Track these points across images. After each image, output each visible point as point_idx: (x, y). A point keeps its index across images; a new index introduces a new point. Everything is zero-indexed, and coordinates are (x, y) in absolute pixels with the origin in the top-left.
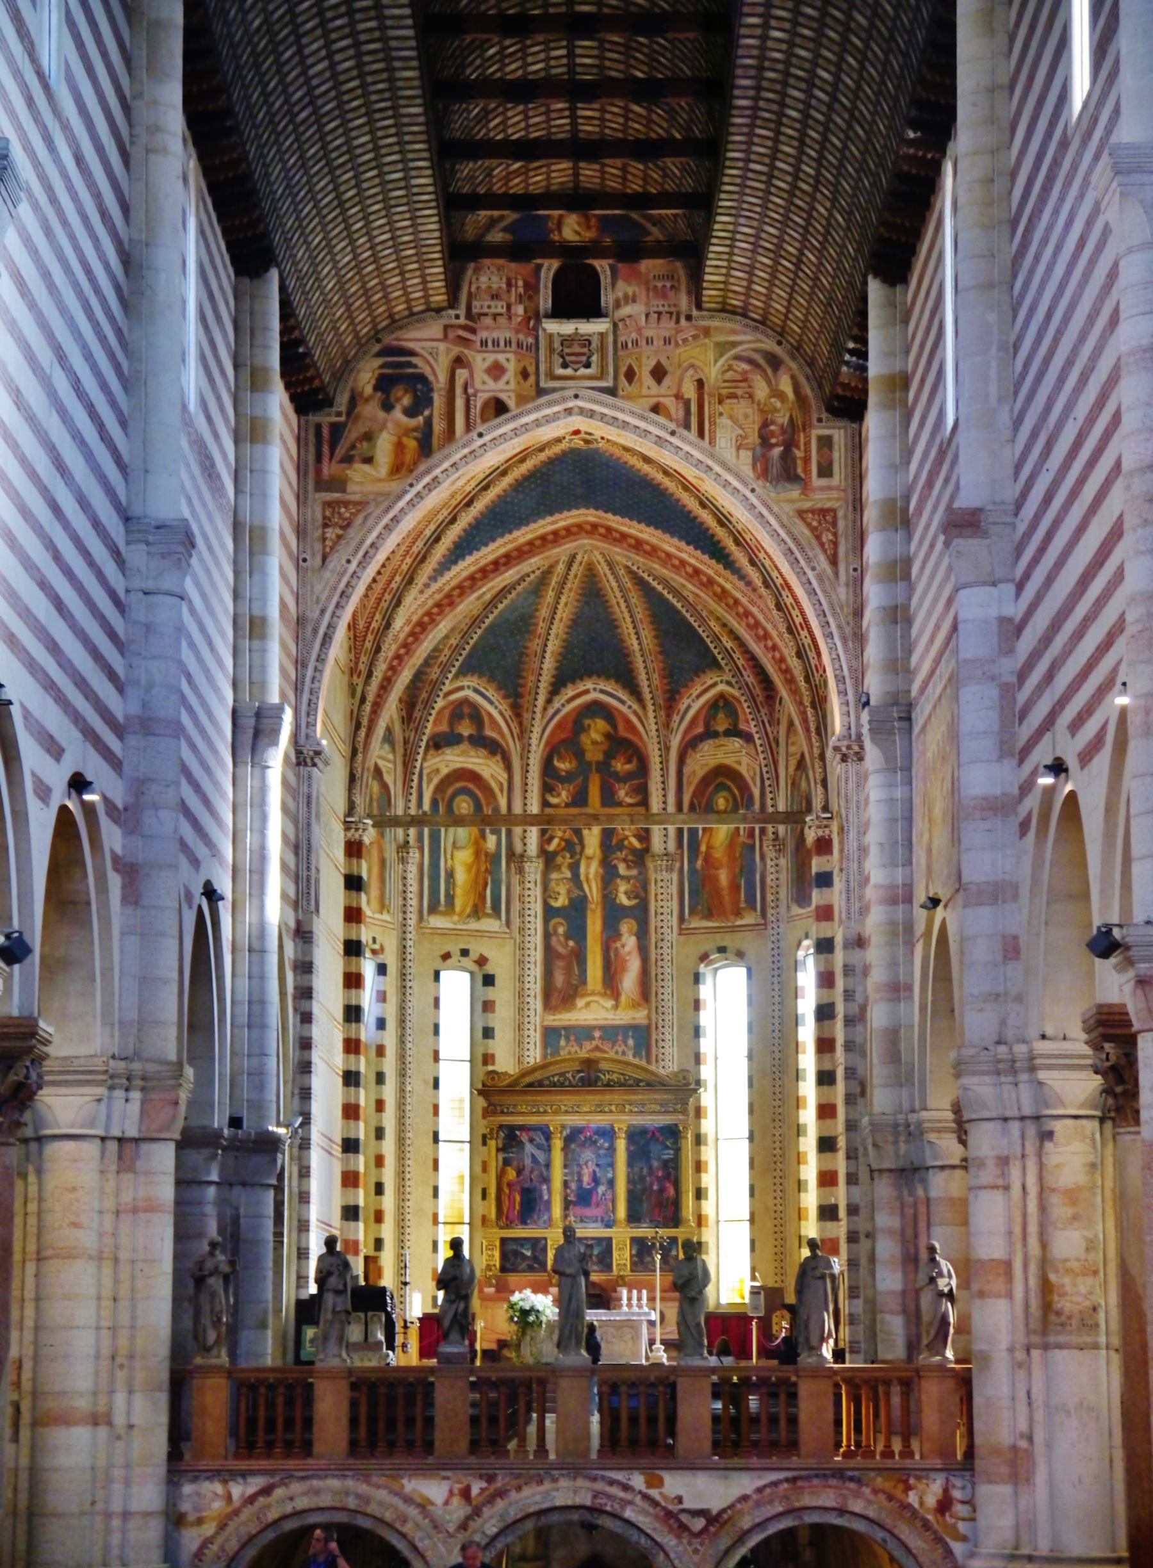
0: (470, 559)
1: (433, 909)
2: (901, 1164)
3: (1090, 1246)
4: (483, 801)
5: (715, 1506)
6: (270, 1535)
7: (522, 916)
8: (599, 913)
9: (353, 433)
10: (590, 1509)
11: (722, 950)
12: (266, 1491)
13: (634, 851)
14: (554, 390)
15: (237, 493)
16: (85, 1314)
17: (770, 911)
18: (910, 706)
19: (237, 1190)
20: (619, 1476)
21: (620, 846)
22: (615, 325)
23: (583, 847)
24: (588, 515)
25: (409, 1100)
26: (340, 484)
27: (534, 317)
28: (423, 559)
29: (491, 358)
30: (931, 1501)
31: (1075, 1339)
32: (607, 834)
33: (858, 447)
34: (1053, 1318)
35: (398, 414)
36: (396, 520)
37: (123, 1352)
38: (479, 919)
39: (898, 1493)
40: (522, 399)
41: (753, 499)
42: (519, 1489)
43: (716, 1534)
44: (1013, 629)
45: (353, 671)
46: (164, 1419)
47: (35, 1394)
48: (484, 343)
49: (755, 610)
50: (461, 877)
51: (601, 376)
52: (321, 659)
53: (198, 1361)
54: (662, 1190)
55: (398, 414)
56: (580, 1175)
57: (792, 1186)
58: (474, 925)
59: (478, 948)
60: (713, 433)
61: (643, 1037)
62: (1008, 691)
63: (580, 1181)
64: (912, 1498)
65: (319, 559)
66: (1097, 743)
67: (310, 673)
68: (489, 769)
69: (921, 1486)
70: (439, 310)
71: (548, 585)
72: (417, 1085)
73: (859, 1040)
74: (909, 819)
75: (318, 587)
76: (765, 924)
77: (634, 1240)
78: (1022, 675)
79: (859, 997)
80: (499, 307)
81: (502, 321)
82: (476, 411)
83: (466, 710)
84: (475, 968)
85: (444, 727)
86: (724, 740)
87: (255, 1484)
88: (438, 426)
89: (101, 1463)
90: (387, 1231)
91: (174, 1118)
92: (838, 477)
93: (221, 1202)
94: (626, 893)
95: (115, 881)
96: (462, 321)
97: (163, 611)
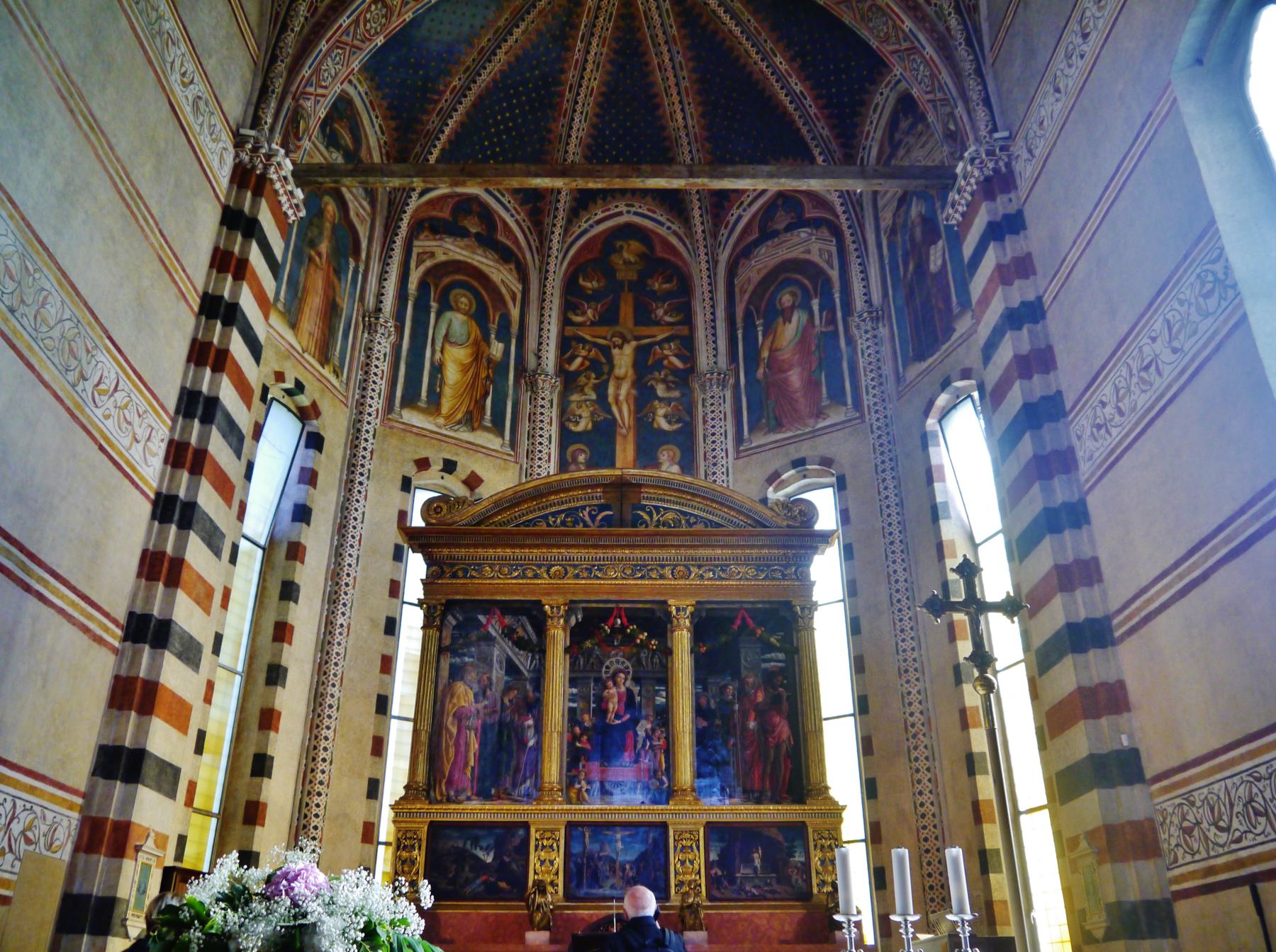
1: (410, 400)
4: (489, 304)
7: (531, 436)
8: (631, 437)
11: (799, 463)
13: (675, 371)
17: (867, 400)
21: (659, 365)
23: (612, 367)
25: (338, 638)
32: (642, 355)
38: (473, 429)
54: (766, 728)
56: (602, 702)
58: (465, 435)
63: (601, 711)
68: (501, 275)
71: (576, 27)
76: (862, 417)
83: (475, 207)
85: (445, 214)
86: (784, 237)
94: (665, 416)
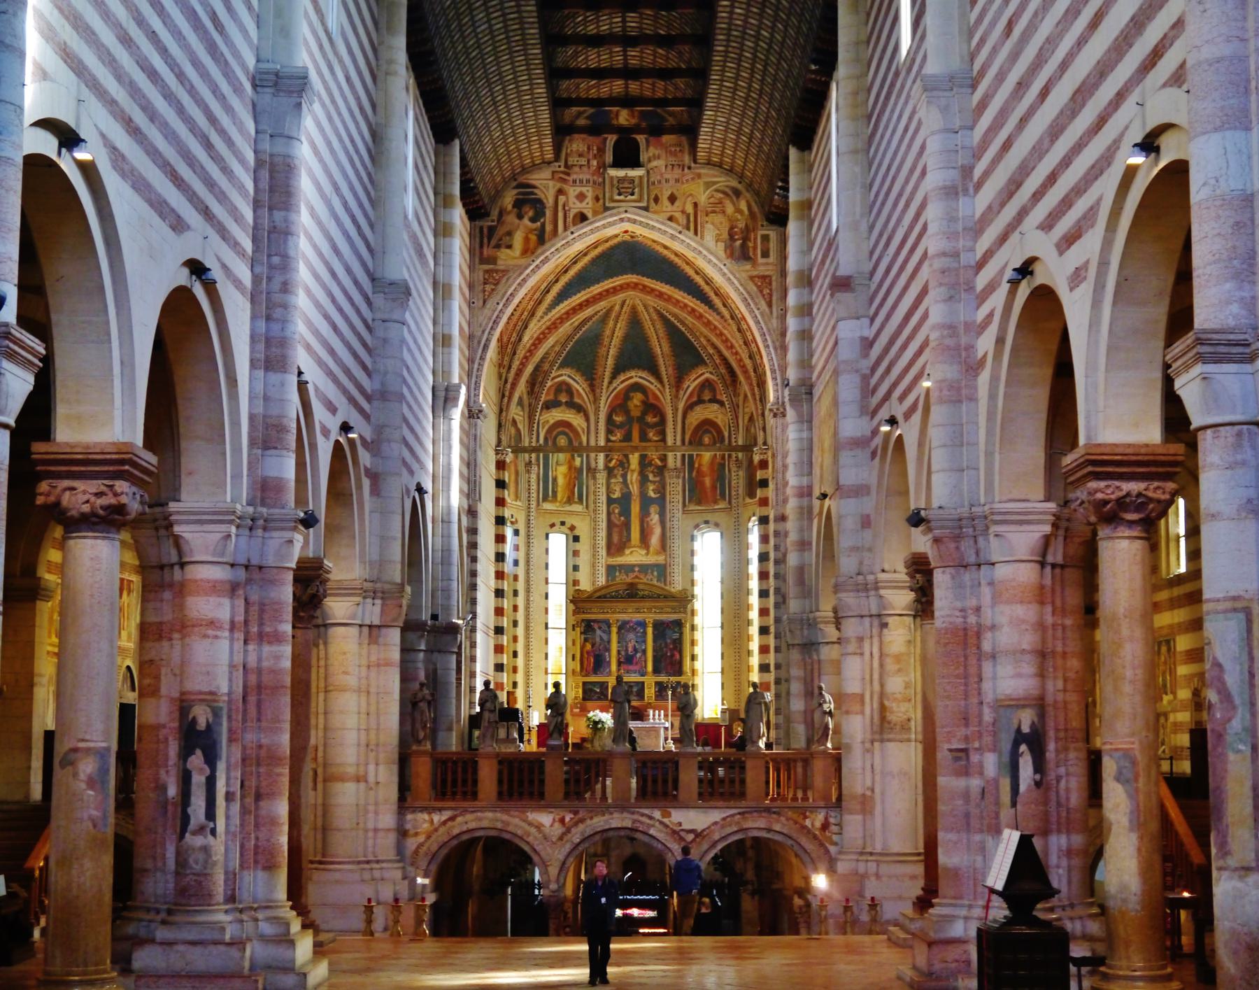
0: (566, 303)
1: (545, 499)
2: (805, 641)
3: (907, 686)
5: (699, 827)
6: (455, 842)
9: (501, 231)
10: (631, 829)
11: (707, 522)
12: (452, 819)
13: (657, 467)
14: (613, 208)
15: (435, 265)
16: (351, 721)
18: (811, 386)
19: (436, 655)
20: (646, 811)
21: (650, 464)
22: (648, 172)
24: (632, 278)
26: (493, 260)
27: (603, 166)
28: (540, 302)
29: (578, 189)
30: (818, 824)
31: (899, 737)
32: (643, 458)
33: (783, 241)
34: (886, 725)
35: (526, 221)
36: (524, 280)
37: (373, 742)
39: (800, 820)
40: (595, 213)
41: (726, 271)
42: (591, 818)
43: (700, 843)
44: (868, 344)
45: (500, 365)
46: (395, 779)
47: (325, 765)
48: (574, 181)
49: (725, 332)
50: (561, 481)
51: (640, 200)
52: (482, 358)
53: (414, 748)
54: (673, 656)
55: (526, 221)
57: (744, 654)
58: (568, 508)
59: (570, 521)
60: (702, 232)
61: (662, 571)
62: (865, 379)
63: (627, 650)
64: (808, 823)
65: (481, 302)
66: (913, 408)
67: (476, 366)
68: (577, 420)
69: (813, 816)
70: (549, 163)
72: (536, 597)
73: (782, 572)
74: (811, 450)
75: (481, 318)
77: (657, 683)
78: (873, 369)
79: (782, 548)
80: (583, 161)
81: (585, 169)
82: (570, 220)
84: (568, 532)
85: (551, 397)
87: (446, 815)
88: (549, 228)
89: (362, 802)
90: (520, 678)
91: (400, 614)
92: (773, 258)
93: (427, 661)
95: (366, 482)
96: (562, 169)
97: (393, 331)
